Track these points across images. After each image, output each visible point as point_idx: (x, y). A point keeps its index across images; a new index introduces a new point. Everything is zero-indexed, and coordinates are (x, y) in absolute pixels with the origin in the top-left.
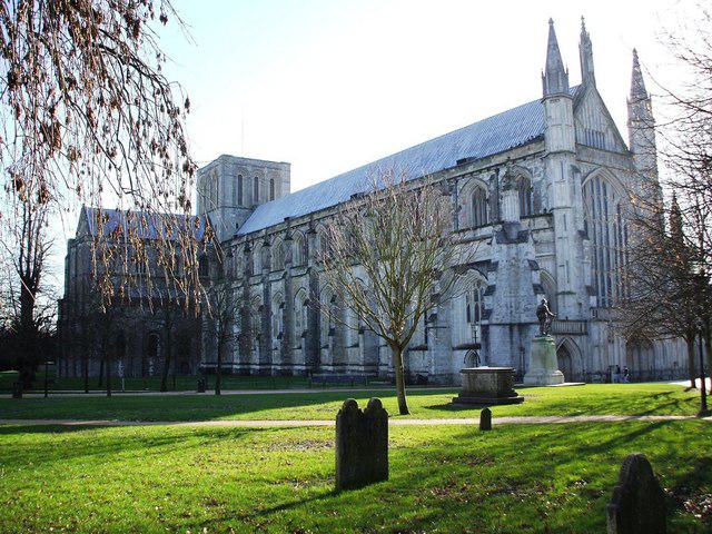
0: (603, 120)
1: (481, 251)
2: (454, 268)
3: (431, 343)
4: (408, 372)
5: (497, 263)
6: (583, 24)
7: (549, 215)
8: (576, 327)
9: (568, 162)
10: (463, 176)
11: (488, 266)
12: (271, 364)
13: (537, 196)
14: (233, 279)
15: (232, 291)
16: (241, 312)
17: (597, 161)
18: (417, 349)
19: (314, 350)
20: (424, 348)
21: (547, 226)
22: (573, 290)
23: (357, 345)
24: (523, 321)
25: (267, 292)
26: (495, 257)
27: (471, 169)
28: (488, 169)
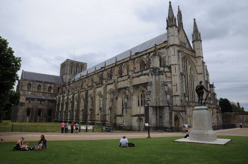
0: (185, 39)
1: (143, 79)
2: (134, 86)
3: (124, 114)
4: (115, 124)
5: (151, 82)
6: (179, 8)
7: (170, 67)
8: (181, 109)
9: (177, 49)
10: (137, 57)
11: (145, 85)
12: (73, 120)
13: (165, 62)
14: (64, 93)
15: (64, 97)
16: (66, 103)
17: (184, 51)
18: (119, 116)
19: (85, 115)
20: (121, 116)
21: (169, 71)
22: (179, 95)
23: (98, 114)
24: (161, 105)
25: (73, 97)
26: (151, 80)
27: (140, 55)
28: (146, 54)
